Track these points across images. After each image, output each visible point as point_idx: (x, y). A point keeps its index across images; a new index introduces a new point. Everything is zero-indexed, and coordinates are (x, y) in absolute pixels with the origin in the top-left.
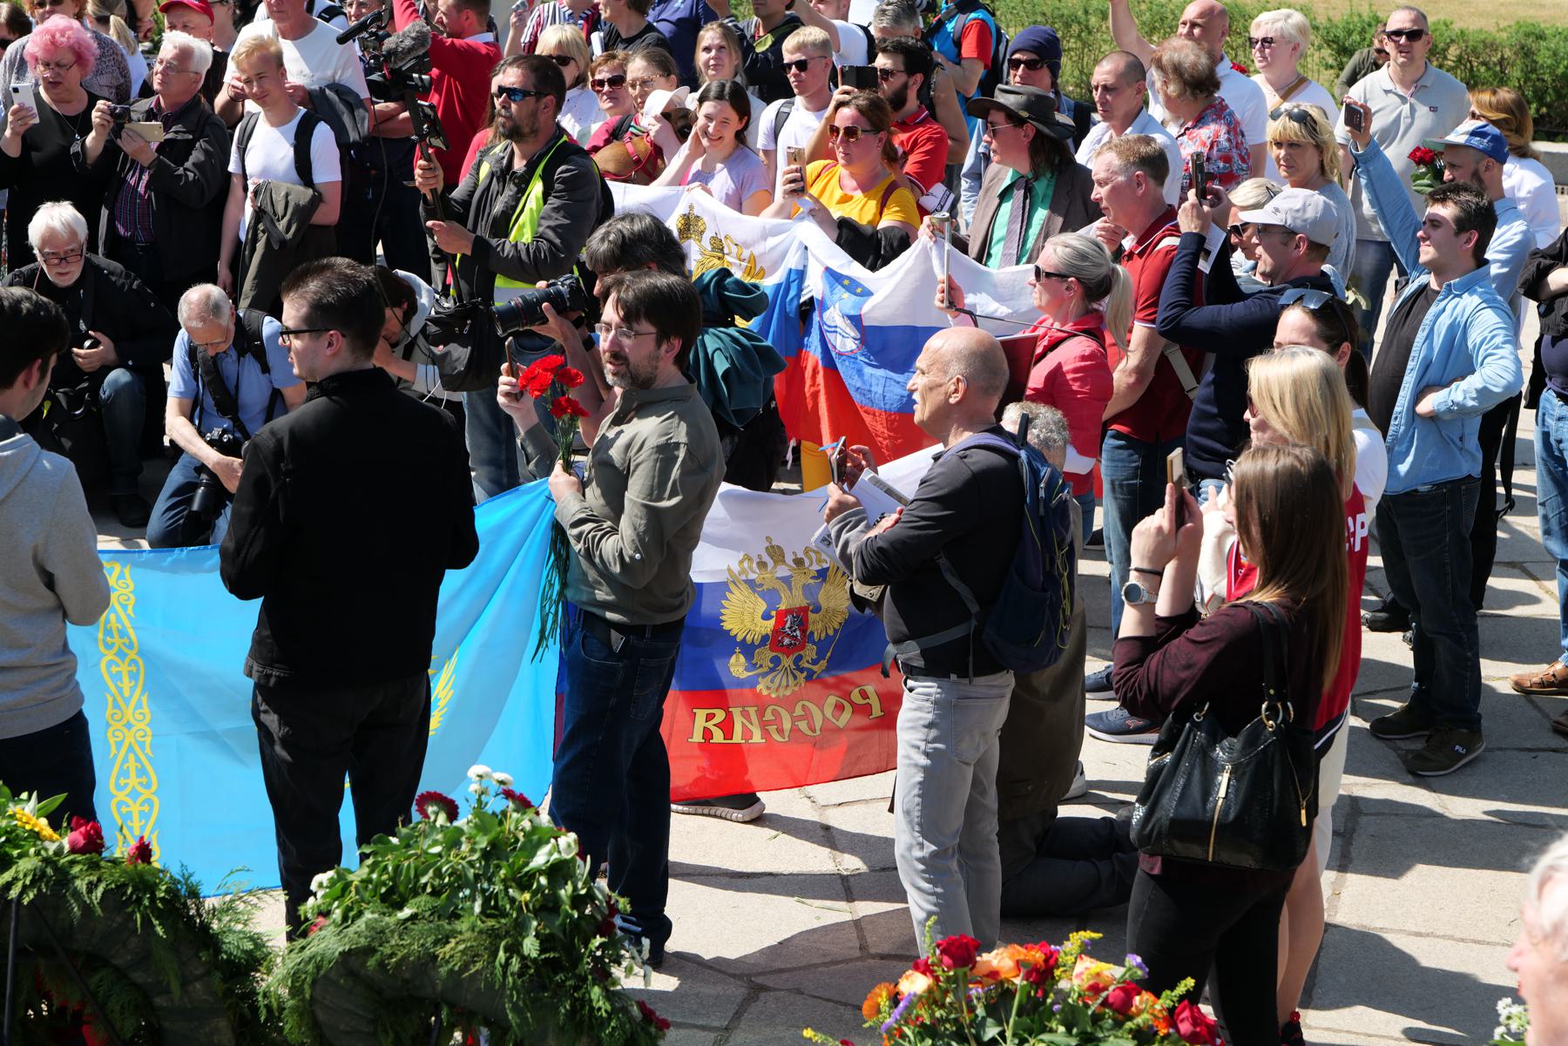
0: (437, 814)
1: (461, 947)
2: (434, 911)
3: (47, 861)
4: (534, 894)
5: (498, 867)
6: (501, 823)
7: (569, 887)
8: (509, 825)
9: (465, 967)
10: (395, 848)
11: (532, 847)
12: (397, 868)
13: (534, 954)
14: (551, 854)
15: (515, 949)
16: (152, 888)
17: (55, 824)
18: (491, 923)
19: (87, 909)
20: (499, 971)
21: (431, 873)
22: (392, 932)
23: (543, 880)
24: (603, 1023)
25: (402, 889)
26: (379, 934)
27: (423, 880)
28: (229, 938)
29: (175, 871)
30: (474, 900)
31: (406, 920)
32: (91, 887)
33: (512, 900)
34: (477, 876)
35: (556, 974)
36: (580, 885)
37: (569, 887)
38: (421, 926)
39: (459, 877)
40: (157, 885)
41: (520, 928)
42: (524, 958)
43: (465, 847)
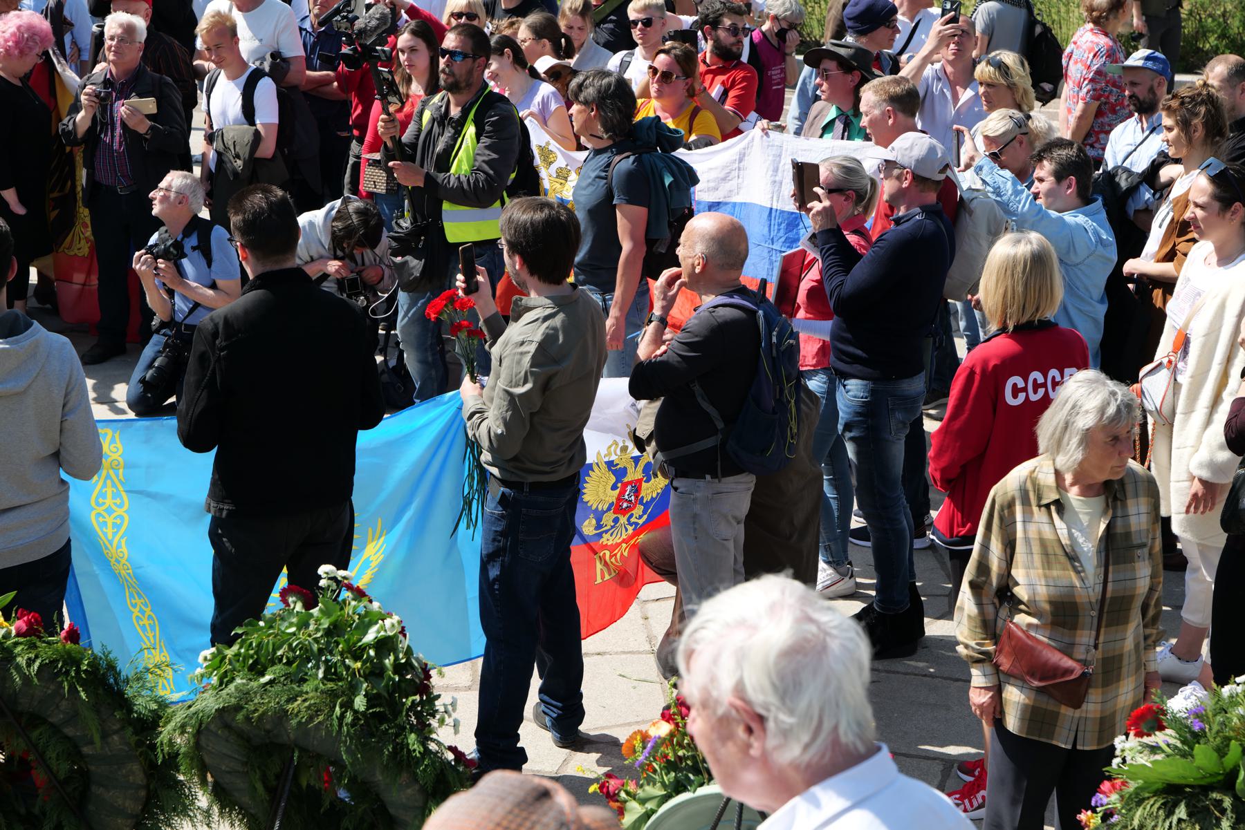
0: (295, 603)
1: (307, 704)
2: (287, 676)
4: (364, 663)
5: (338, 644)
6: (342, 609)
7: (392, 658)
8: (349, 610)
9: (311, 718)
10: (262, 628)
11: (364, 627)
12: (259, 645)
13: (362, 709)
14: (378, 632)
15: (348, 705)
16: (78, 663)
18: (330, 685)
19: (26, 679)
20: (336, 722)
21: (286, 646)
22: (255, 693)
23: (372, 653)
24: (418, 762)
25: (263, 660)
26: (246, 695)
27: (279, 653)
28: (140, 701)
30: (318, 668)
31: (266, 684)
32: (30, 662)
33: (348, 668)
34: (320, 650)
35: (381, 724)
36: (401, 656)
37: (392, 658)
38: (278, 688)
39: (307, 650)
40: (82, 659)
41: (353, 689)
42: (356, 712)
43: (312, 627)
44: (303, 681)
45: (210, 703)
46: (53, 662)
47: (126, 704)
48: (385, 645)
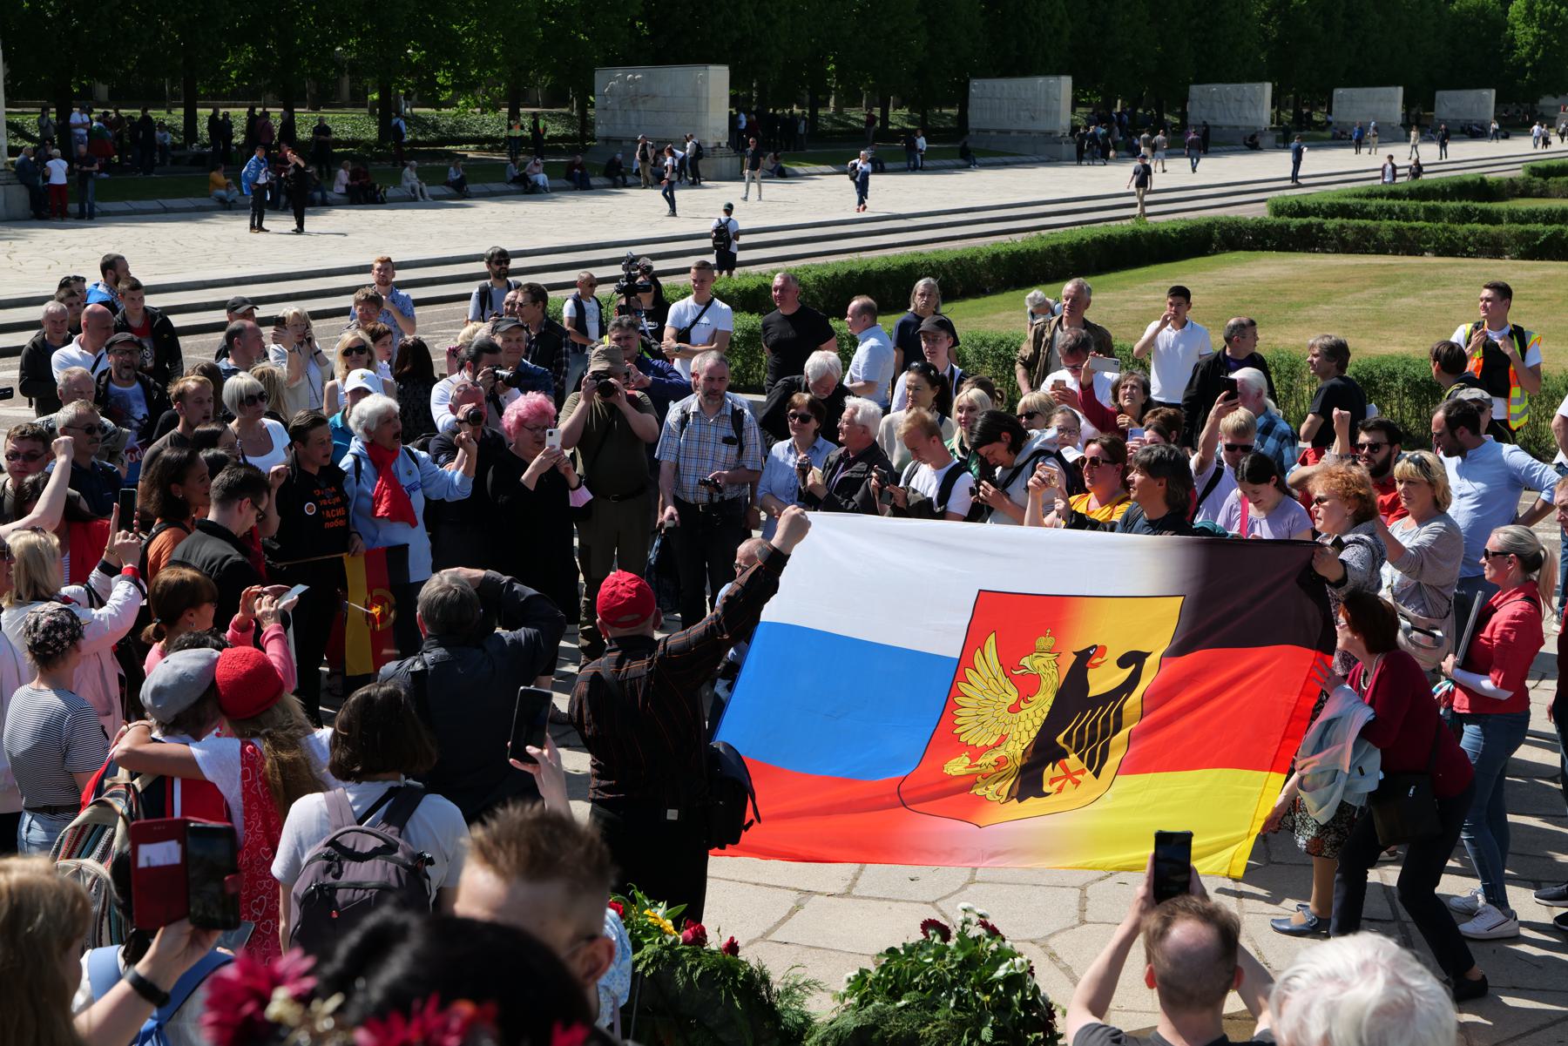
3: (665, 948)
4: (993, 997)
8: (982, 946)
12: (898, 972)
15: (975, 1035)
16: (736, 973)
17: (677, 928)
18: (960, 1015)
26: (882, 1016)
28: (788, 1014)
29: (753, 964)
33: (977, 1000)
38: (913, 1013)
41: (981, 1021)
44: (935, 1008)
45: (851, 1022)
46: (713, 971)
48: (1015, 981)
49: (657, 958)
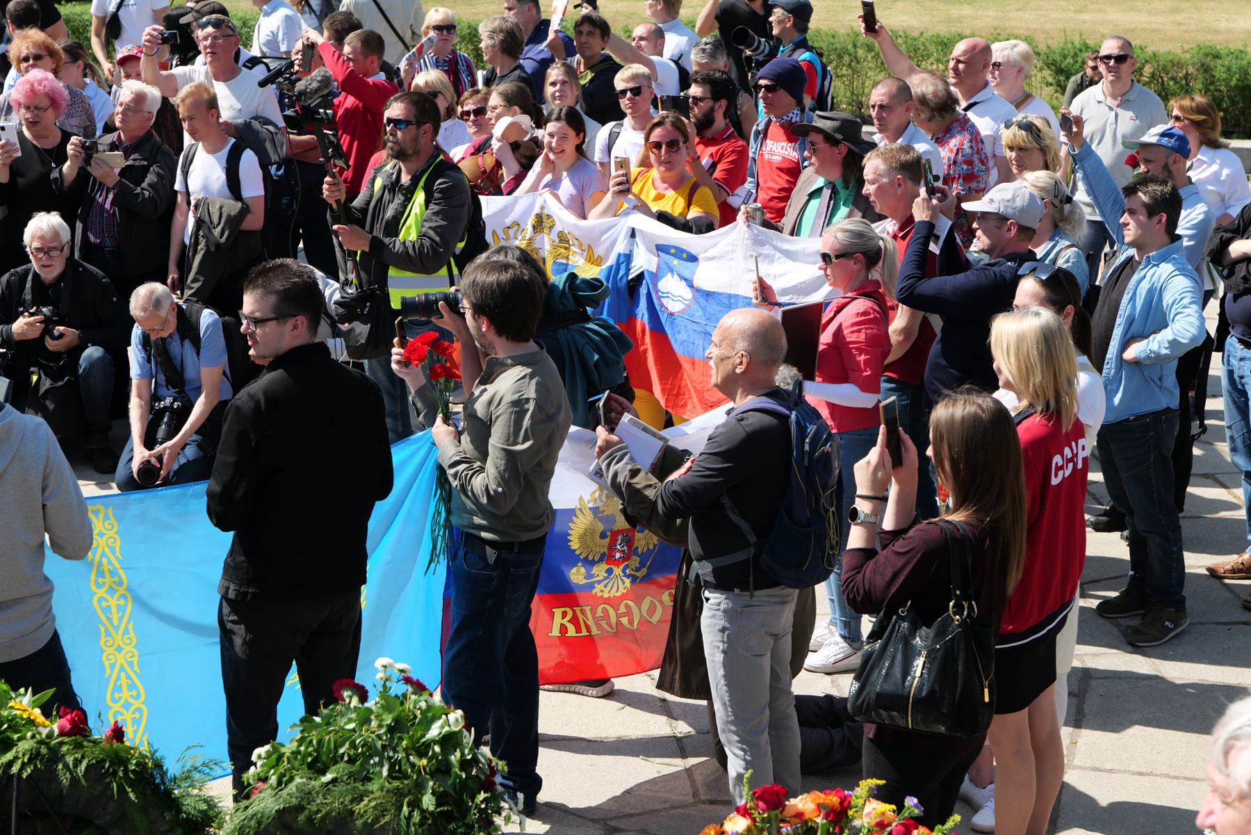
0: (351, 697)
1: (373, 804)
3: (41, 742)
4: (430, 760)
5: (401, 739)
6: (402, 704)
7: (458, 754)
8: (409, 705)
9: (377, 820)
10: (318, 725)
11: (428, 722)
12: (320, 742)
13: (431, 808)
14: (442, 727)
15: (416, 804)
16: (124, 762)
17: (47, 713)
18: (396, 784)
19: (74, 780)
20: (403, 822)
21: (347, 745)
22: (318, 793)
23: (437, 749)
25: (324, 758)
26: (307, 795)
27: (341, 751)
29: (144, 749)
30: (382, 766)
31: (329, 783)
32: (77, 762)
33: (413, 765)
34: (384, 747)
35: (450, 823)
36: (466, 751)
37: (458, 754)
38: (340, 787)
39: (370, 748)
40: (128, 760)
41: (419, 787)
42: (423, 811)
43: (374, 724)
44: (368, 779)
46: (100, 762)
47: (174, 804)
49: (34, 756)
